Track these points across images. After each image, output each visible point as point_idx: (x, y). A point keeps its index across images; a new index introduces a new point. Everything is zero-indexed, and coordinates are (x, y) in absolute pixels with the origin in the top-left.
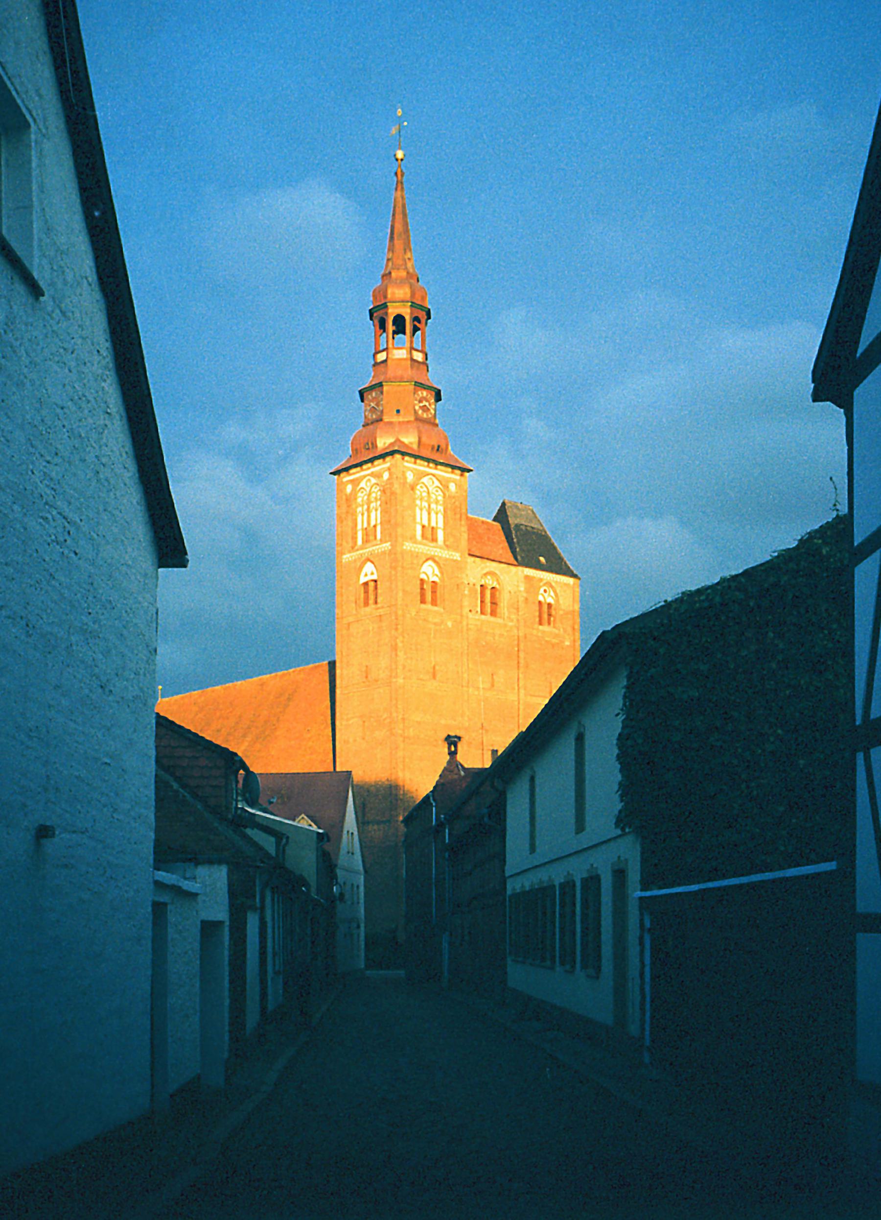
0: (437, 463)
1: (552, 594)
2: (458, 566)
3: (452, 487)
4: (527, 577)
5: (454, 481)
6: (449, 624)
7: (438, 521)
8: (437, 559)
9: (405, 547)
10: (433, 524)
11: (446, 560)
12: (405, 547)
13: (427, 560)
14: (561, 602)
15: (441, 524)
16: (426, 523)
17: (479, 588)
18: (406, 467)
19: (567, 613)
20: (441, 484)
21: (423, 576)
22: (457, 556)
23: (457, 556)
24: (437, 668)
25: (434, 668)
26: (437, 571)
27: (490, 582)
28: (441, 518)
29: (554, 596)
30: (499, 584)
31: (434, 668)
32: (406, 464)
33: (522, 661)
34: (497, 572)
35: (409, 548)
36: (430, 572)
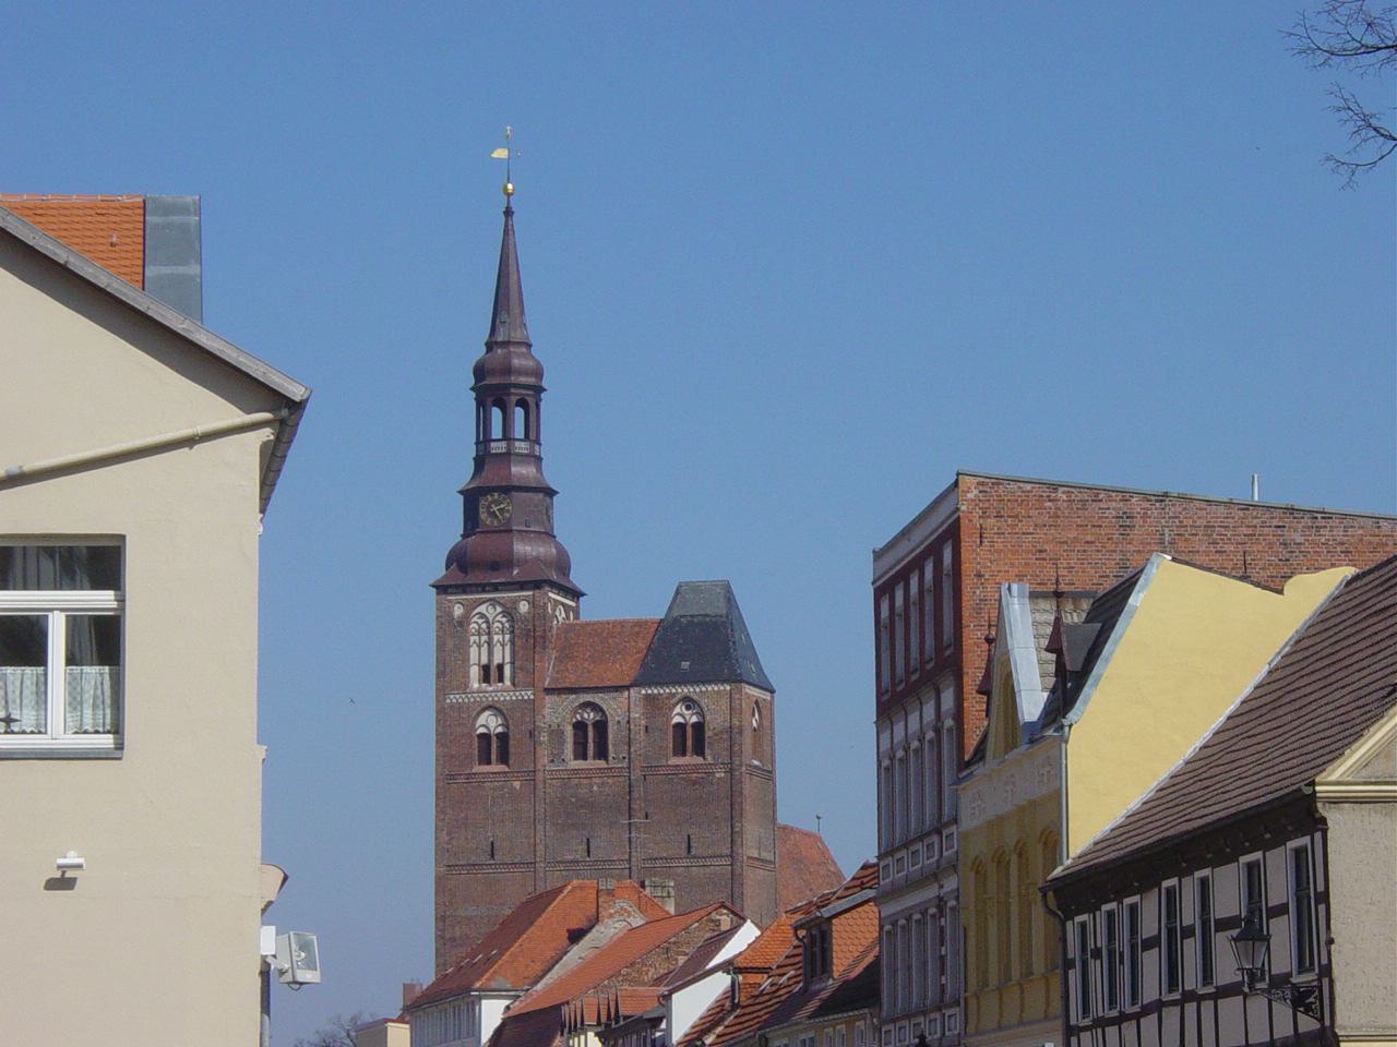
2: (532, 707)
3: (524, 607)
6: (517, 785)
7: (502, 654)
8: (498, 706)
10: (497, 660)
11: (512, 702)
12: (448, 701)
13: (484, 710)
14: (708, 718)
16: (484, 660)
17: (569, 731)
18: (450, 601)
21: (482, 730)
22: (528, 694)
23: (528, 694)
25: (492, 843)
31: (492, 843)
36: (489, 723)
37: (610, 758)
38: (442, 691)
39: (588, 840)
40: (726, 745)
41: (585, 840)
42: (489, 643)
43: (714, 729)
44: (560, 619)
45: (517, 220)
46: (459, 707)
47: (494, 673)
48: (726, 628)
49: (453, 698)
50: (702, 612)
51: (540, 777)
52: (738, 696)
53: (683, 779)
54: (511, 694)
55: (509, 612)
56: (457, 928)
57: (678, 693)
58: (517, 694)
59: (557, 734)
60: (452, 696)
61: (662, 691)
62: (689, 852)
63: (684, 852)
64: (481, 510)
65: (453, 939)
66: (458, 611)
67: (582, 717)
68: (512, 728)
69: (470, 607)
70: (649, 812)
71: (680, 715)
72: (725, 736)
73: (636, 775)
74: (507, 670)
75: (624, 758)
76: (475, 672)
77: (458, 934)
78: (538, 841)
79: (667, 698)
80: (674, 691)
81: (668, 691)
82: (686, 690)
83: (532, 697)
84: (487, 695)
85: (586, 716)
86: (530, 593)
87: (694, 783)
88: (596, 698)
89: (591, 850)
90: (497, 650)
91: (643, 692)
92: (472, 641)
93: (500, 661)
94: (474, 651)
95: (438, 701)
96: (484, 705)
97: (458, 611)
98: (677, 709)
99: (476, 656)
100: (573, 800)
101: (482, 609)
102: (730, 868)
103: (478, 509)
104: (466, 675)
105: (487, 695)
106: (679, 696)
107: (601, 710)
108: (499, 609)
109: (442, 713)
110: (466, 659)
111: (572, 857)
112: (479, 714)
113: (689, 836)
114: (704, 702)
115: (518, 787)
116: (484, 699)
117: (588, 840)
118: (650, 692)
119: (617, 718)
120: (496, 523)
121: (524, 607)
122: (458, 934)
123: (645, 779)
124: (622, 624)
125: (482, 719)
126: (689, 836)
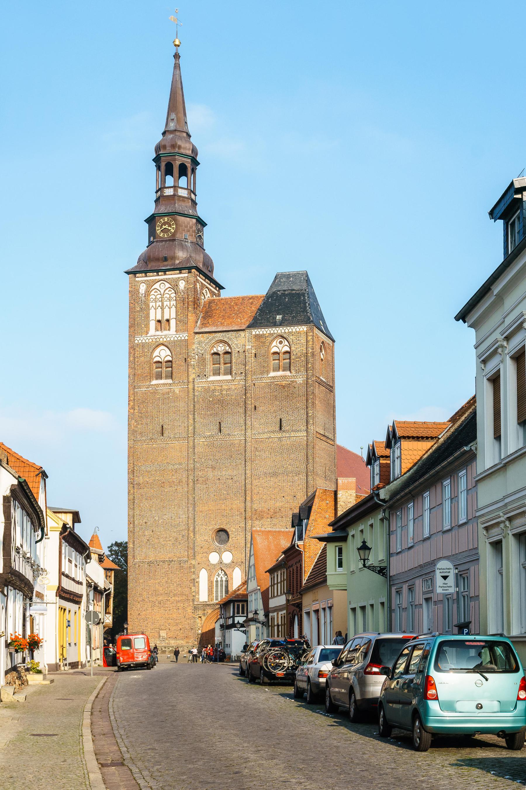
0: (165, 271)
1: (286, 343)
2: (186, 344)
3: (182, 285)
4: (256, 336)
5: (183, 279)
7: (170, 313)
8: (166, 344)
9: (136, 342)
10: (166, 317)
11: (174, 342)
12: (136, 342)
13: (158, 346)
14: (293, 348)
15: (173, 315)
16: (159, 317)
18: (138, 282)
20: (171, 285)
21: (157, 359)
22: (184, 336)
24: (165, 427)
26: (168, 353)
27: (221, 348)
28: (173, 310)
29: (289, 345)
30: (230, 348)
32: (137, 279)
33: (249, 407)
34: (226, 339)
35: (140, 341)
37: (234, 374)
38: (132, 336)
39: (220, 423)
40: (304, 363)
42: (162, 309)
43: (297, 354)
44: (206, 297)
45: (181, 61)
46: (143, 345)
47: (164, 322)
48: (304, 296)
49: (139, 339)
50: (290, 288)
52: (311, 334)
53: (278, 384)
54: (174, 336)
55: (174, 286)
56: (141, 478)
57: (275, 333)
58: (177, 336)
59: (202, 360)
60: (138, 339)
61: (265, 332)
62: (281, 429)
63: (278, 428)
64: (157, 228)
65: (139, 484)
66: (143, 288)
67: (217, 350)
68: (174, 357)
69: (150, 285)
71: (276, 347)
74: (173, 323)
75: (242, 373)
76: (153, 325)
77: (141, 481)
78: (190, 424)
80: (272, 332)
81: (268, 332)
82: (279, 331)
83: (186, 338)
84: (159, 337)
85: (219, 349)
86: (186, 275)
87: (284, 387)
89: (222, 428)
90: (166, 310)
91: (254, 333)
92: (151, 306)
93: (168, 318)
94: (152, 312)
95: (130, 341)
96: (157, 344)
97: (143, 288)
98: (274, 344)
99: (154, 315)
100: (211, 399)
101: (157, 286)
102: (305, 438)
103: (156, 229)
104: (147, 326)
105: (159, 337)
106: (275, 335)
107: (229, 345)
108: (168, 285)
109: (132, 348)
110: (148, 316)
112: (154, 349)
113: (281, 419)
115: (178, 392)
116: (158, 340)
118: (257, 333)
119: (238, 350)
120: (166, 236)
121: (182, 285)
122: (141, 481)
124: (243, 298)
125: (156, 353)
126: (281, 419)
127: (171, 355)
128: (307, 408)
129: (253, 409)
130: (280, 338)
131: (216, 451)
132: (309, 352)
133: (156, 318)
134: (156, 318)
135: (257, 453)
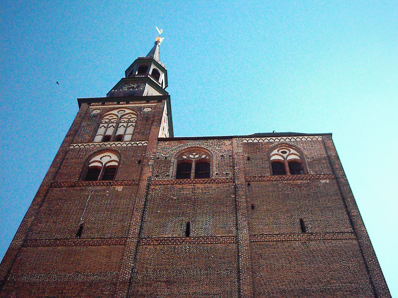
1: (292, 151)
4: (248, 144)
14: (305, 153)
15: (130, 130)
17: (174, 161)
19: (319, 160)
26: (114, 157)
39: (188, 225)
41: (184, 224)
51: (144, 184)
70: (257, 203)
72: (324, 161)
73: (241, 180)
79: (265, 144)
83: (145, 144)
88: (203, 145)
98: (275, 152)
101: (115, 112)
111: (170, 235)
114: (300, 146)
117: (188, 225)
123: (249, 185)
127: (117, 160)
128: (346, 207)
129: (250, 208)
130: (283, 149)
131: (180, 258)
132: (333, 156)
133: (105, 133)
134: (105, 133)
135: (262, 261)
